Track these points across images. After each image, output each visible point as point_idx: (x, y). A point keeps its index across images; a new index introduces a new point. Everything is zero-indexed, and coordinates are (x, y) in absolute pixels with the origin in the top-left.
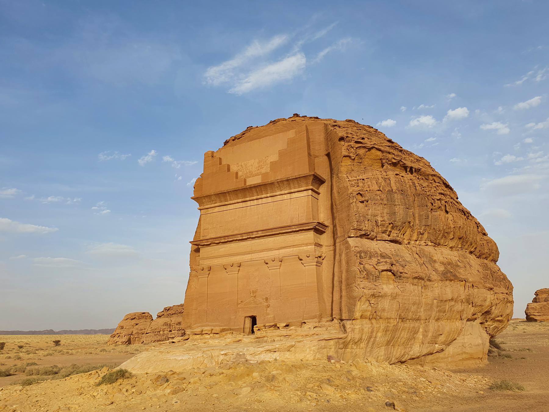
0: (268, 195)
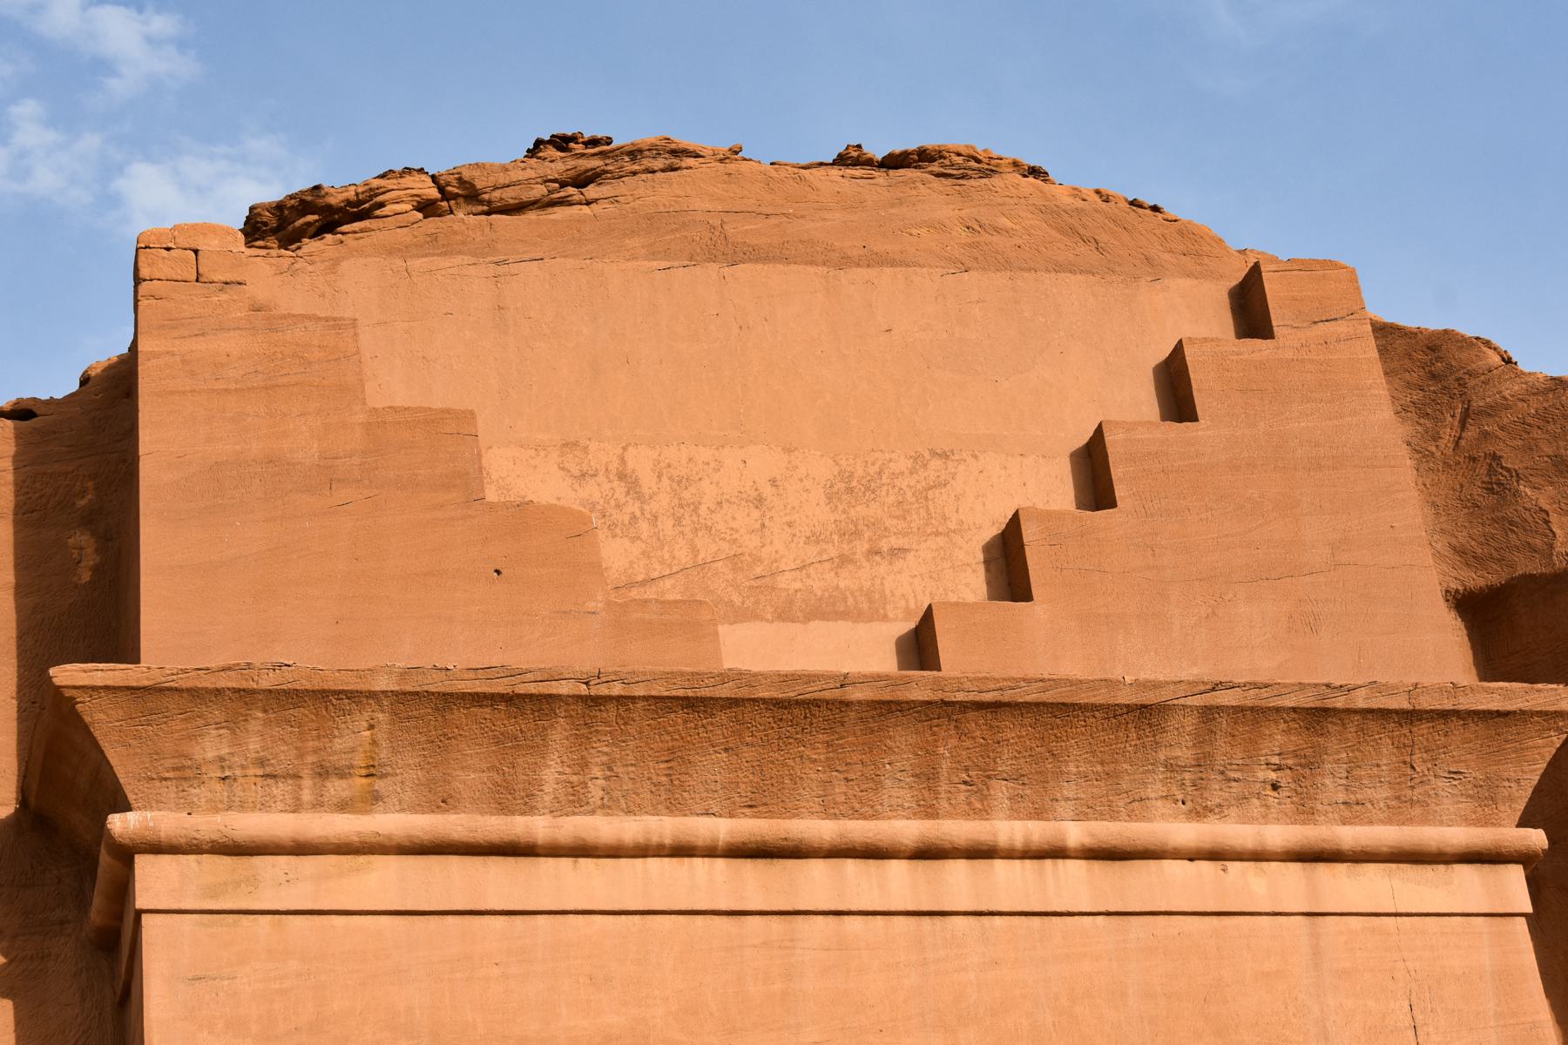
0: (1075, 833)
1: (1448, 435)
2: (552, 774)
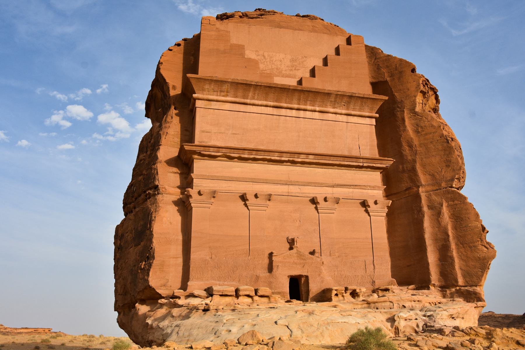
0: (318, 109)
1: (373, 61)
2: (251, 94)
